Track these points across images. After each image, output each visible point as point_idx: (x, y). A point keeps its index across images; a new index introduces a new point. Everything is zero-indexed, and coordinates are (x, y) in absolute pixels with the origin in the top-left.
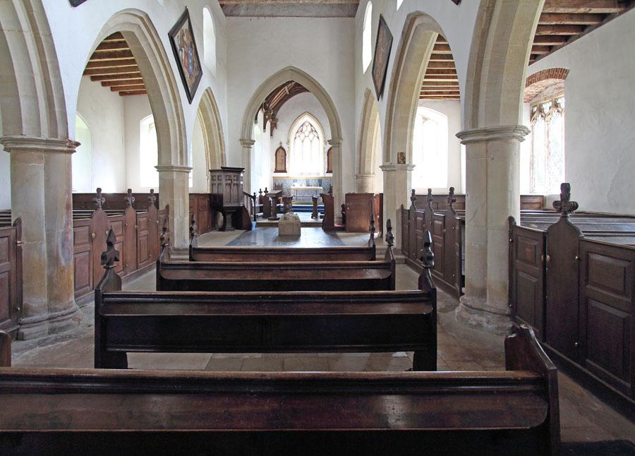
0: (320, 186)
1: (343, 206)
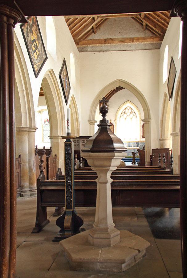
0: (138, 146)
1: (151, 156)
